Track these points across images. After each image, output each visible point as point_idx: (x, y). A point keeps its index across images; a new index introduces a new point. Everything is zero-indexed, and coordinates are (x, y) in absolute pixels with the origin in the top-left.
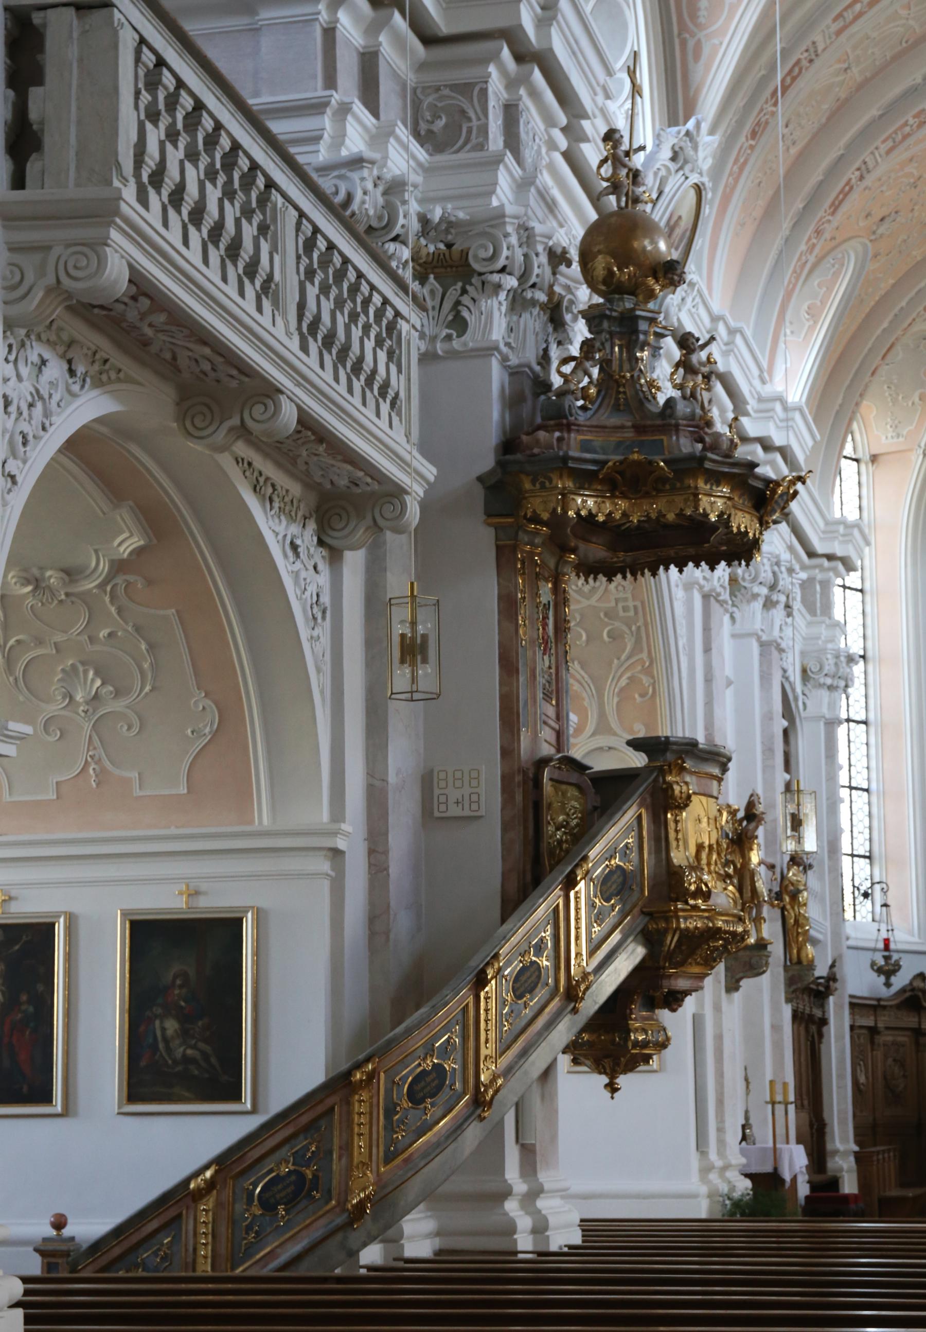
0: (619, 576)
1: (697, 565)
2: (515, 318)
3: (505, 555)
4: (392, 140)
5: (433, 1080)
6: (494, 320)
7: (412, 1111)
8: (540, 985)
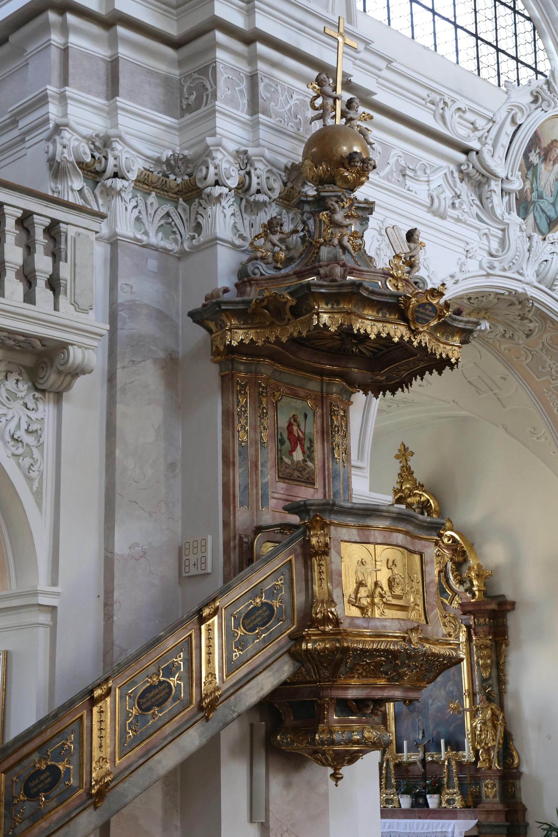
0: (400, 390)
1: (431, 373)
2: (253, 217)
3: (227, 382)
4: (119, 112)
5: (46, 779)
6: (224, 220)
7: (28, 803)
8: (170, 700)
